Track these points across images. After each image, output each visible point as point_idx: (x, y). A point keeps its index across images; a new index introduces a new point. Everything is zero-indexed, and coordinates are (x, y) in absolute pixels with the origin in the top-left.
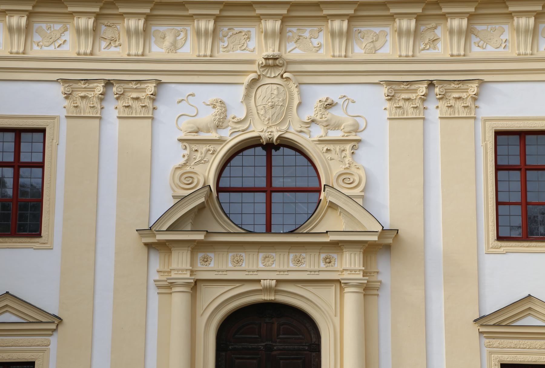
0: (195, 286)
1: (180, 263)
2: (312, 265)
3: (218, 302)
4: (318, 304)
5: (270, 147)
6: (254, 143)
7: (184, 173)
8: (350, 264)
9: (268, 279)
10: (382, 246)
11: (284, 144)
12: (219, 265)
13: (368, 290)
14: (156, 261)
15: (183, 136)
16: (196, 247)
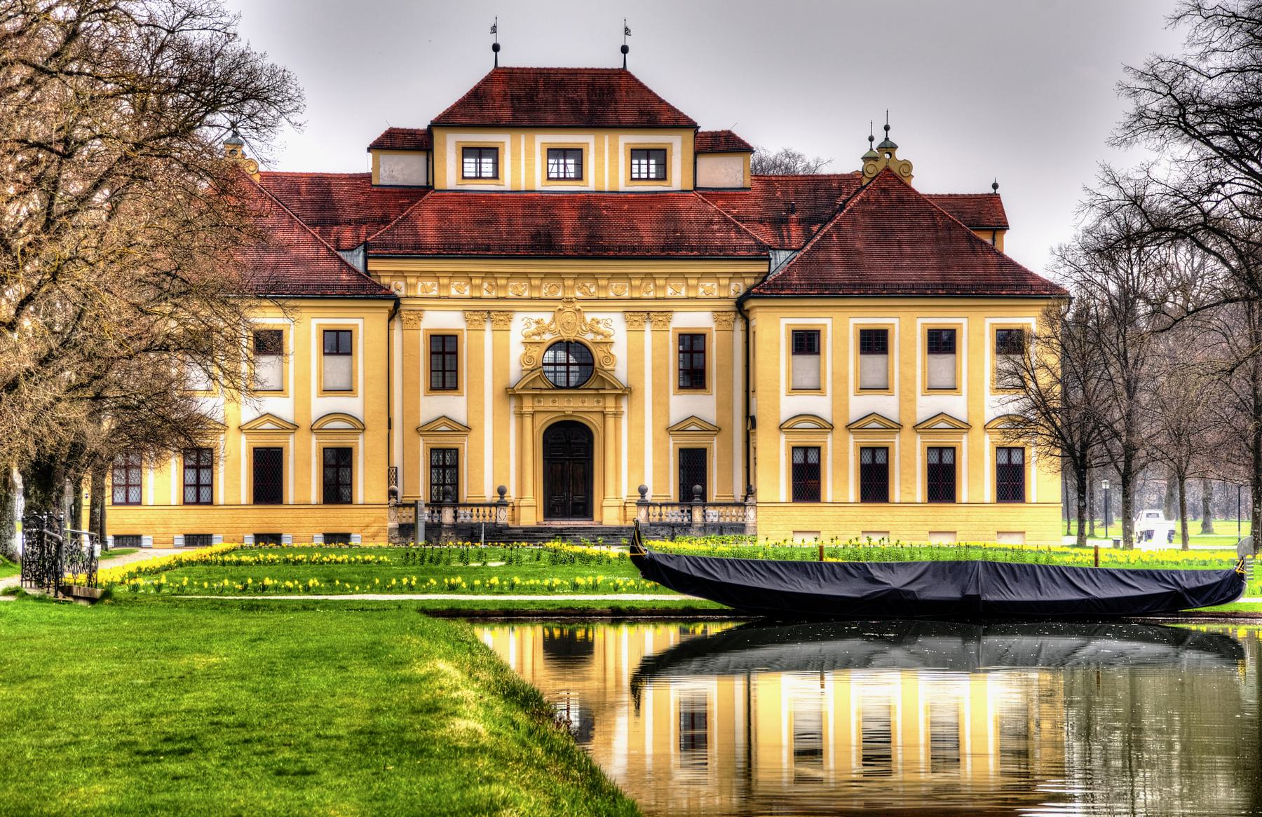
0: (533, 414)
1: (528, 406)
2: (590, 404)
3: (543, 421)
4: (594, 421)
5: (568, 342)
6: (560, 342)
7: (527, 358)
8: (610, 404)
9: (569, 411)
10: (625, 393)
11: (577, 342)
12: (547, 404)
13: (617, 415)
14: (513, 403)
15: (523, 339)
16: (534, 396)
